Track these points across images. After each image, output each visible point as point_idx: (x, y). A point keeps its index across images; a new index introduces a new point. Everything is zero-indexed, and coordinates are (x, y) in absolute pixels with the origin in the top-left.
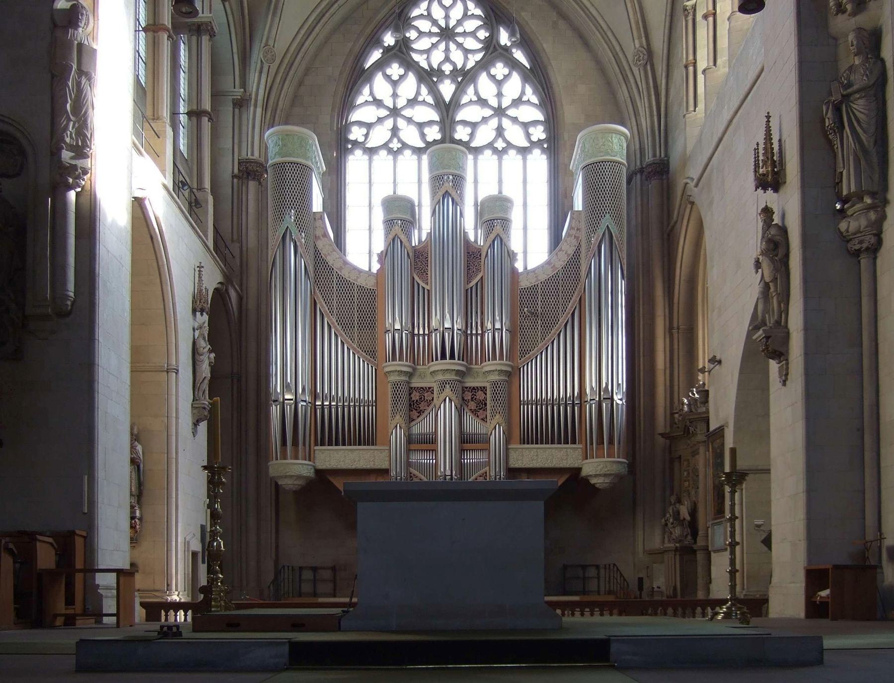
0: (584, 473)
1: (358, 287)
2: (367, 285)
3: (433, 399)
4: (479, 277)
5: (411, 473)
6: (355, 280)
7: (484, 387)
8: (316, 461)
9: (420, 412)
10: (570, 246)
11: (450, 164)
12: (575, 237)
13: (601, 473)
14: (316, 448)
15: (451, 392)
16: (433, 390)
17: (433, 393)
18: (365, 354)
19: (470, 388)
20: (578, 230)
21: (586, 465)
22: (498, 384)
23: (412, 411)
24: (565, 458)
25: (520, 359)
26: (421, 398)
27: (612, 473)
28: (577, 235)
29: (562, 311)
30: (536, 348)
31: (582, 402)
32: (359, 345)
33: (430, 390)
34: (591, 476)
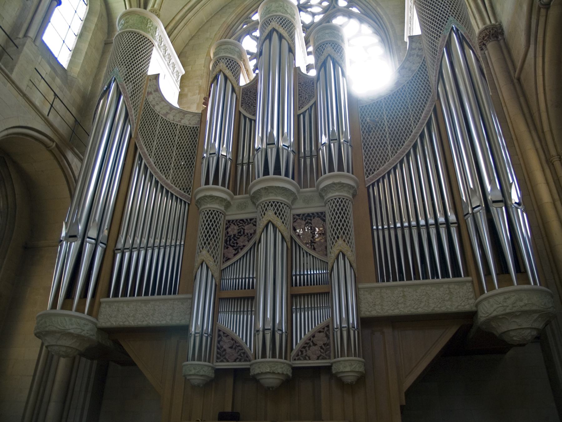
0: (482, 316)
1: (181, 127)
2: (190, 124)
3: (255, 231)
4: (312, 102)
5: (219, 331)
6: (180, 121)
7: (322, 213)
8: (101, 317)
9: (237, 250)
10: (414, 63)
11: (277, 10)
12: (417, 55)
13: (515, 309)
14: (102, 300)
15: (275, 216)
16: (256, 222)
17: (255, 225)
18: (178, 189)
19: (304, 215)
20: (419, 49)
21: (485, 303)
22: (338, 202)
23: (227, 248)
24: (447, 298)
25: (367, 177)
26: (240, 232)
27: (534, 308)
28: (419, 54)
29: (415, 122)
30: (387, 163)
31: (461, 216)
32: (174, 181)
33: (252, 222)
34: (496, 317)
